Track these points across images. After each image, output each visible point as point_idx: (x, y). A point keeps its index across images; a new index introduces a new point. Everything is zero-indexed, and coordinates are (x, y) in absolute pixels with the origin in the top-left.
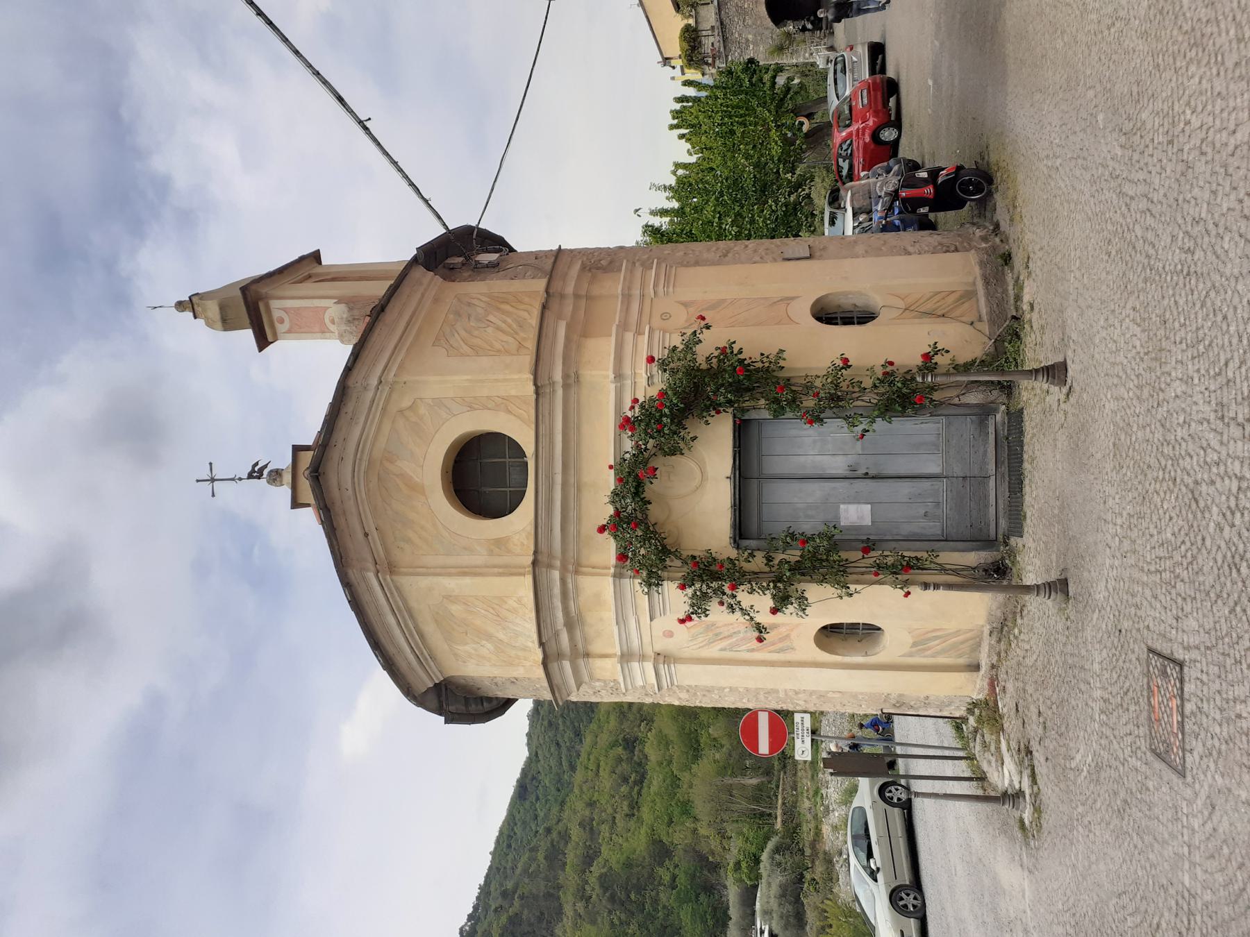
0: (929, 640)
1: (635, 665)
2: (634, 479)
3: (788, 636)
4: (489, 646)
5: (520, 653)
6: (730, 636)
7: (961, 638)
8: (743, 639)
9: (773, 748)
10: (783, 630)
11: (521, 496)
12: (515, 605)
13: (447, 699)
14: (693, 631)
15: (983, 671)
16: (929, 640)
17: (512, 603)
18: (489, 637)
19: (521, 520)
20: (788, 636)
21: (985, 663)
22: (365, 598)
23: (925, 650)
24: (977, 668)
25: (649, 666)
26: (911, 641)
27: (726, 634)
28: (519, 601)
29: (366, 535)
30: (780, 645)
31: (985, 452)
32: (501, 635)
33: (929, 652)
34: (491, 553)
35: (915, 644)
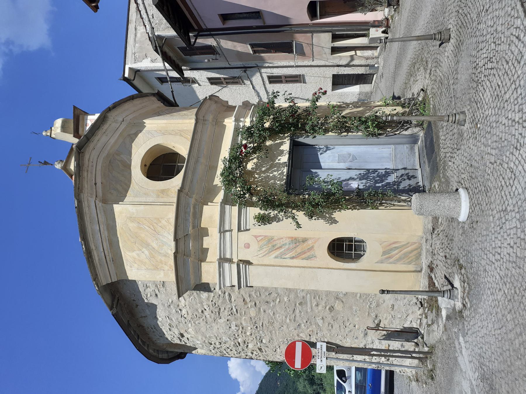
0: (391, 250)
1: (227, 265)
2: (238, 158)
3: (312, 247)
4: (146, 252)
5: (163, 259)
6: (281, 247)
7: (410, 249)
8: (288, 249)
9: (303, 364)
10: (310, 242)
11: (178, 172)
12: (166, 224)
13: (117, 306)
14: (261, 243)
15: (423, 272)
16: (391, 250)
17: (164, 222)
18: (147, 245)
19: (177, 181)
20: (312, 247)
21: (425, 267)
22: (86, 210)
23: (390, 258)
24: (420, 271)
25: (234, 267)
26: (381, 250)
27: (279, 245)
28: (168, 221)
29: (96, 184)
30: (308, 254)
31: (415, 160)
32: (154, 245)
33: (391, 260)
34: (158, 196)
35: (384, 253)
